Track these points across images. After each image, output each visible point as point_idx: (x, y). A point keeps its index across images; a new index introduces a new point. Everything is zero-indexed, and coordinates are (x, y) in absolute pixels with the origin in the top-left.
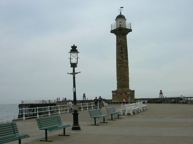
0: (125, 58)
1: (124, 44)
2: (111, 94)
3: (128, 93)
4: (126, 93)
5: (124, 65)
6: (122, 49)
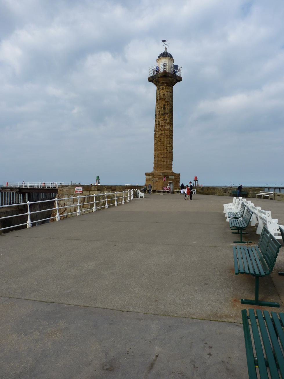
1: (169, 100)
2: (144, 177)
3: (171, 177)
4: (167, 177)
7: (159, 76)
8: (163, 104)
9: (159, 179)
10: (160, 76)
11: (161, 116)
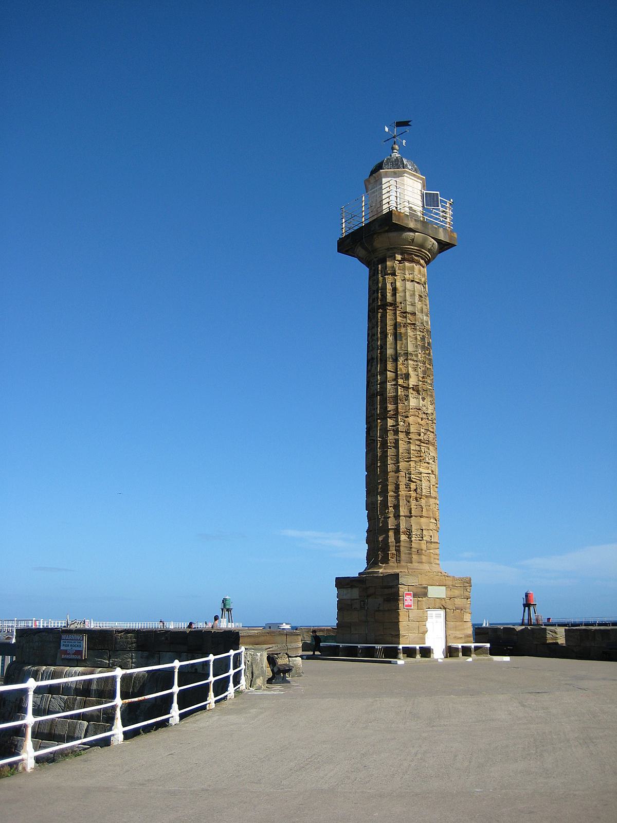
0: (416, 389)
2: (331, 596)
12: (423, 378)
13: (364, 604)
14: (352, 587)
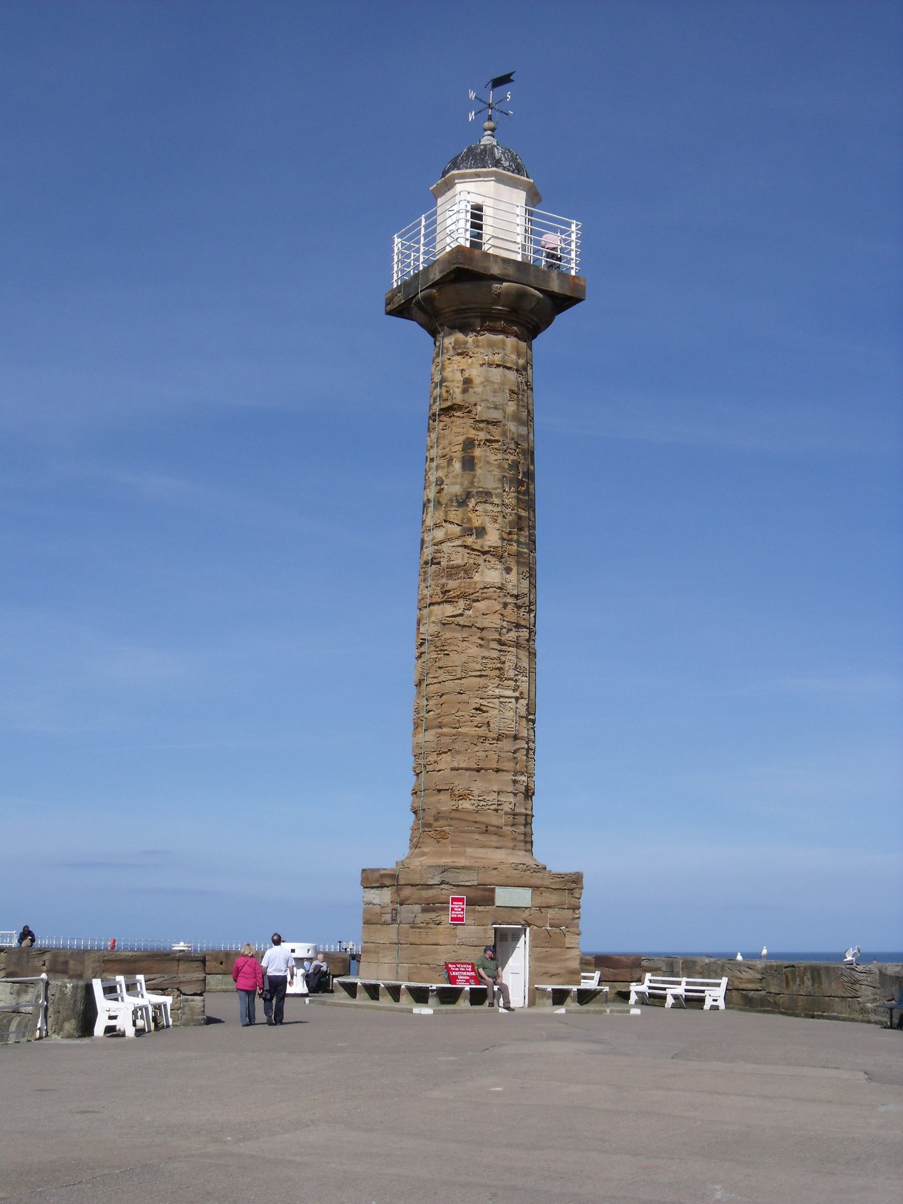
5: (485, 622)
6: (469, 464)
7: (431, 277)
8: (461, 439)
9: (424, 910)
10: (438, 276)
11: (446, 512)
12: (510, 533)
13: (396, 914)
14: (382, 886)
